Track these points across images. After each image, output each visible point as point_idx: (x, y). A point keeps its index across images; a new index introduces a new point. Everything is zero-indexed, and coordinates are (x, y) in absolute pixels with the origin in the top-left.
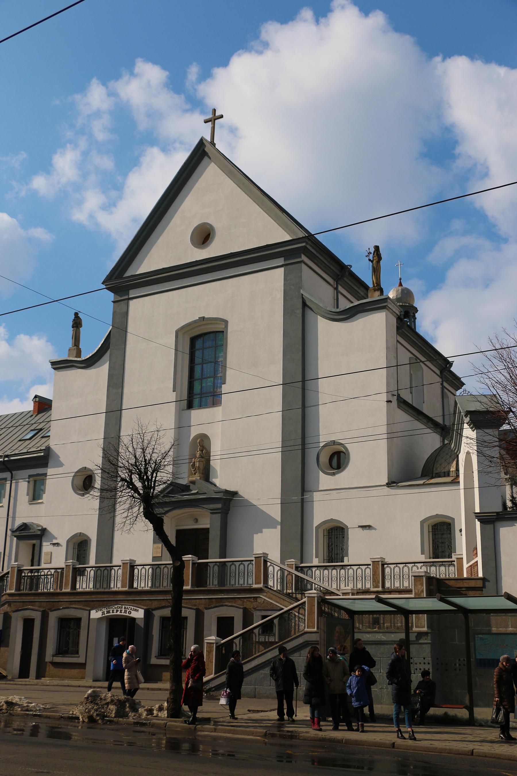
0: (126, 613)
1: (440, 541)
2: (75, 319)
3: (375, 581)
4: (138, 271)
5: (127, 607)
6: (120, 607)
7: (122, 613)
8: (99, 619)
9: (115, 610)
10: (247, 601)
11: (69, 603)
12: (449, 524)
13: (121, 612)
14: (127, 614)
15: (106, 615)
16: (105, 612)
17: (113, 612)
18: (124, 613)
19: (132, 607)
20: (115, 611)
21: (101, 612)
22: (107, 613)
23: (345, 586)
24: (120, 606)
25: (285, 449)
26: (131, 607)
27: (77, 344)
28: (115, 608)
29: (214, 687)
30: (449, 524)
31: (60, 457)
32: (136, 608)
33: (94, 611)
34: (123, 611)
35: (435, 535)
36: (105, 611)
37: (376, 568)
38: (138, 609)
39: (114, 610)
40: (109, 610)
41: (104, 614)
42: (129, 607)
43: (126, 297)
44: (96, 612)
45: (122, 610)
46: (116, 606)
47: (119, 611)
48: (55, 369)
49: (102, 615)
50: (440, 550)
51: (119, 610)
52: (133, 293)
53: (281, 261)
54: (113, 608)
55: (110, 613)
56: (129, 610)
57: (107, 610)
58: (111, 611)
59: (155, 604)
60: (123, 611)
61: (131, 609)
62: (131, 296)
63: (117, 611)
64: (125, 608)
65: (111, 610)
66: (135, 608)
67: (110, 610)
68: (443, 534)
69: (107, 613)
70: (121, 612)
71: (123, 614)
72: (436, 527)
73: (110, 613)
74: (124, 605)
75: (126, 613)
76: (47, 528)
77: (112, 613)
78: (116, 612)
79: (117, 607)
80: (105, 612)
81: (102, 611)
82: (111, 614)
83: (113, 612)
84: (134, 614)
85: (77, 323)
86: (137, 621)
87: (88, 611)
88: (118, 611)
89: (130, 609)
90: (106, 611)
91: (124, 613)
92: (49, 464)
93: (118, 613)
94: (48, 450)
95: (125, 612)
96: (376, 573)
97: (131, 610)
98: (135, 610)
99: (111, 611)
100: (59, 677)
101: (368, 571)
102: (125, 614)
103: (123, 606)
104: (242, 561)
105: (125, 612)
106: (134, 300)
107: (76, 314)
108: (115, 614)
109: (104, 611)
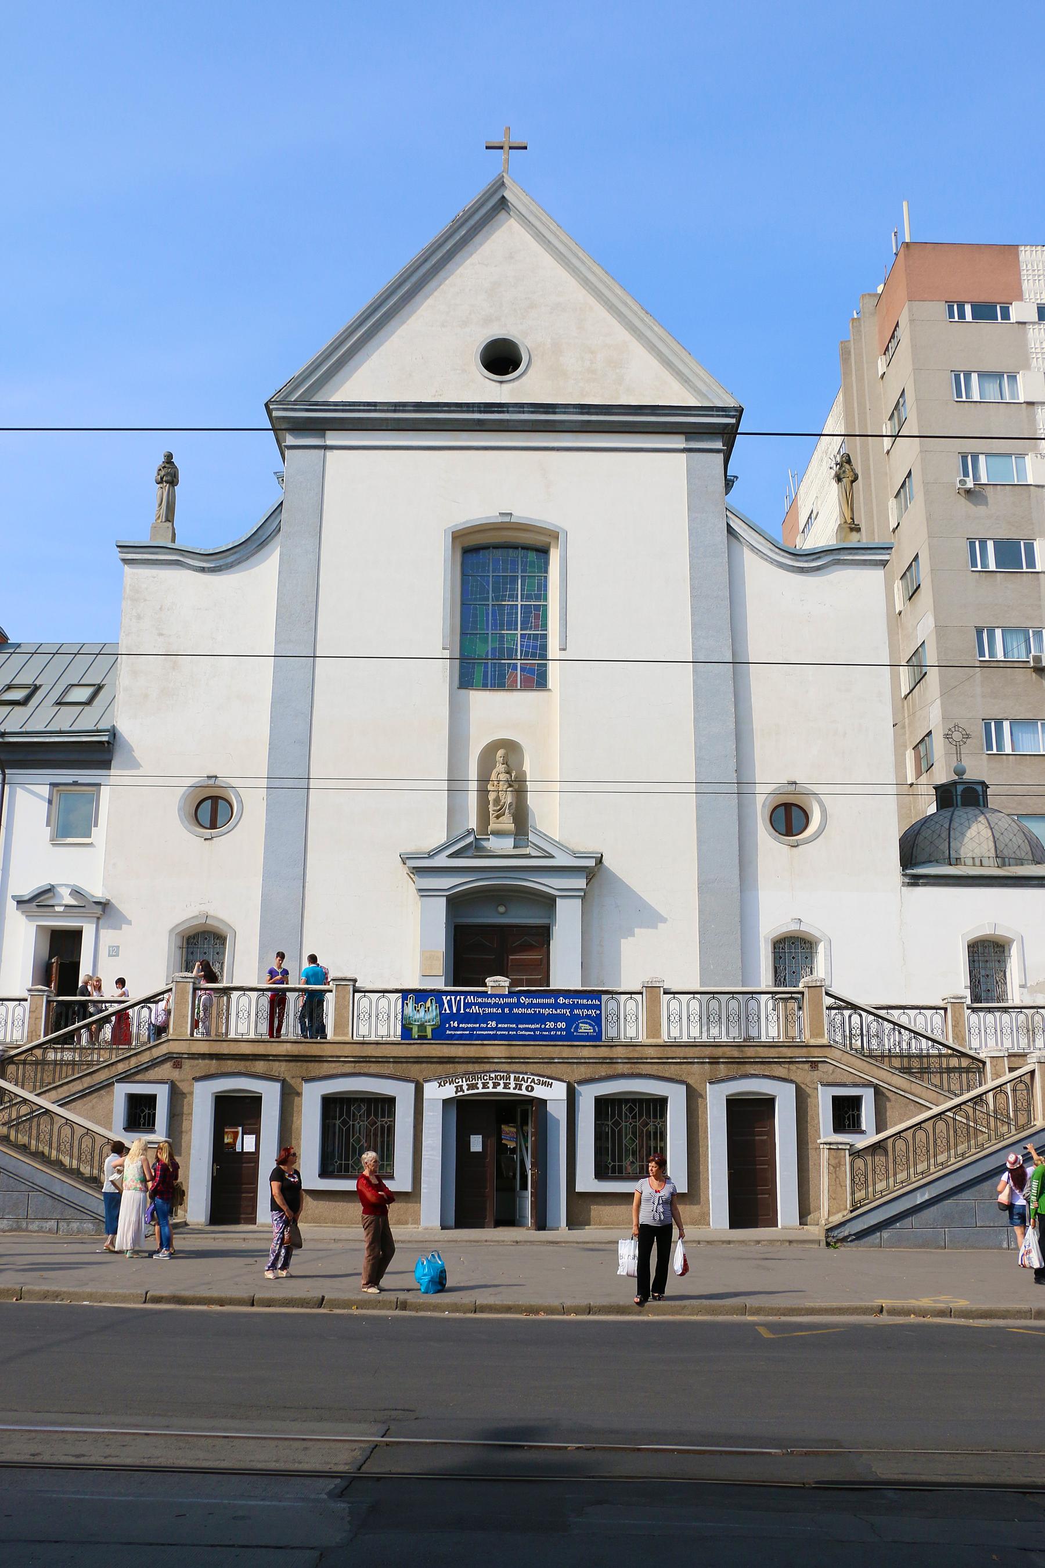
0: (520, 1089)
1: (983, 972)
2: (167, 465)
3: (958, 1037)
4: (334, 396)
5: (521, 1076)
6: (502, 1078)
7: (509, 1088)
8: (446, 1102)
9: (491, 1082)
10: (798, 1068)
11: (353, 1065)
12: (1003, 947)
13: (506, 1086)
14: (524, 1092)
15: (467, 1092)
16: (465, 1087)
17: (485, 1086)
18: (514, 1089)
19: (536, 1078)
20: (491, 1085)
21: (453, 1086)
22: (468, 1090)
23: (997, 1044)
24: (502, 1074)
25: (704, 788)
26: (532, 1077)
27: (169, 519)
28: (490, 1078)
29: (854, 1235)
30: (1003, 947)
31: (135, 749)
32: (545, 1080)
33: (436, 1084)
34: (512, 1085)
35: (974, 961)
36: (465, 1084)
37: (957, 1015)
38: (551, 1081)
39: (488, 1083)
40: (474, 1082)
41: (464, 1092)
42: (526, 1077)
43: (322, 443)
44: (440, 1085)
45: (510, 1084)
46: (493, 1075)
47: (502, 1085)
48: (125, 561)
49: (456, 1093)
50: (983, 987)
51: (501, 1082)
52: (332, 438)
53: (678, 442)
54: (485, 1078)
55: (478, 1089)
56: (529, 1084)
57: (468, 1082)
58: (480, 1085)
59: (583, 1071)
60: (512, 1085)
61: (533, 1081)
62: (329, 443)
63: (495, 1085)
64: (516, 1079)
65: (480, 1082)
66: (541, 1079)
67: (477, 1083)
68: (987, 961)
69: (468, 1090)
70: (506, 1086)
71: (511, 1091)
72: (975, 949)
73: (478, 1089)
74: (513, 1072)
75: (520, 1089)
76: (113, 901)
77: (482, 1088)
78: (494, 1087)
79: (496, 1077)
80: (465, 1087)
81: (455, 1085)
82: (481, 1090)
83: (485, 1086)
84: (540, 1092)
85: (169, 476)
86: (550, 1108)
87: (412, 1086)
88: (499, 1084)
89: (530, 1080)
90: (467, 1085)
91: (514, 1089)
92: (113, 762)
93: (500, 1089)
94: (113, 733)
95: (519, 1086)
96: (958, 1023)
97: (532, 1084)
98: (544, 1083)
99: (480, 1085)
100: (334, 1221)
101: (19, 1010)
102: (517, 1091)
103: (512, 1076)
104: (714, 993)
105: (519, 1086)
106: (335, 452)
107: (169, 457)
108: (491, 1090)
109: (460, 1083)
